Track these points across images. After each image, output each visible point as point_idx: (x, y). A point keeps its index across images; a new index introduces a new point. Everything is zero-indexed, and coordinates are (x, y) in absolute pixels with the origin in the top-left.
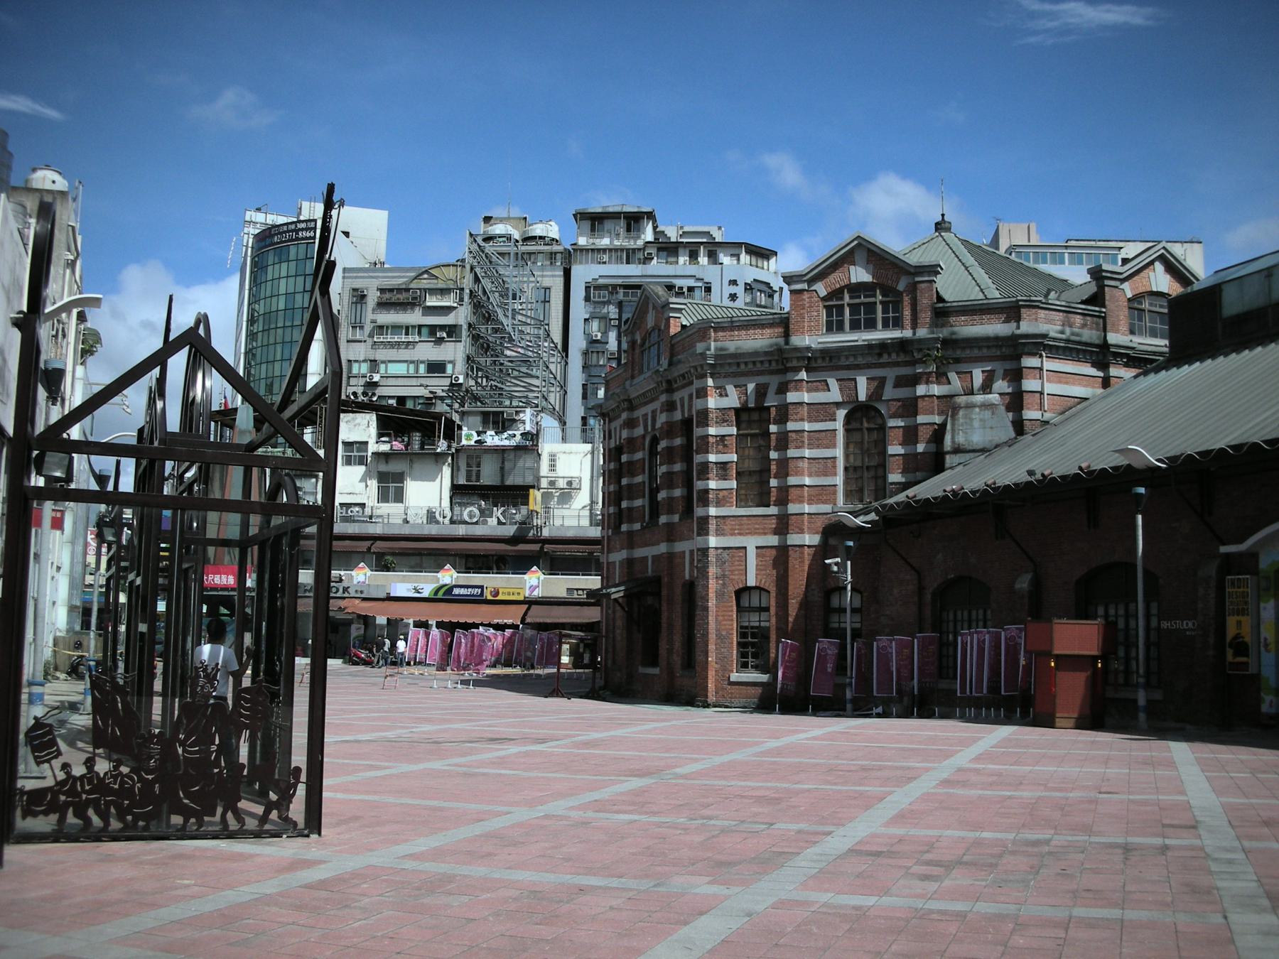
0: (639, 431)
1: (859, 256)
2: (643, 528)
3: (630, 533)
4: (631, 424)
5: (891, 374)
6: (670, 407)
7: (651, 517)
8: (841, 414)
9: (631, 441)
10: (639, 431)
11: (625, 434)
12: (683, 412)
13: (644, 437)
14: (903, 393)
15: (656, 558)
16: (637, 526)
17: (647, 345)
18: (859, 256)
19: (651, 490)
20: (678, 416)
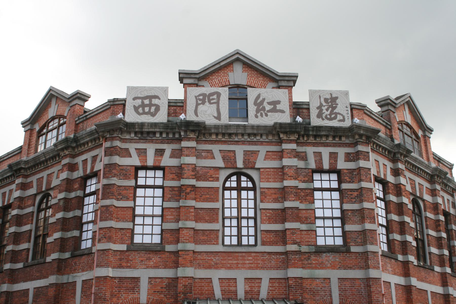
0: (32, 191)
1: (238, 68)
2: (25, 267)
3: (12, 271)
4: (24, 187)
5: (263, 150)
6: (72, 167)
7: (33, 259)
8: (223, 174)
9: (20, 199)
10: (32, 191)
11: (17, 194)
12: (85, 169)
13: (35, 195)
14: (274, 164)
15: (38, 290)
16: (20, 265)
17: (45, 131)
18: (238, 68)
19: (37, 237)
20: (79, 173)
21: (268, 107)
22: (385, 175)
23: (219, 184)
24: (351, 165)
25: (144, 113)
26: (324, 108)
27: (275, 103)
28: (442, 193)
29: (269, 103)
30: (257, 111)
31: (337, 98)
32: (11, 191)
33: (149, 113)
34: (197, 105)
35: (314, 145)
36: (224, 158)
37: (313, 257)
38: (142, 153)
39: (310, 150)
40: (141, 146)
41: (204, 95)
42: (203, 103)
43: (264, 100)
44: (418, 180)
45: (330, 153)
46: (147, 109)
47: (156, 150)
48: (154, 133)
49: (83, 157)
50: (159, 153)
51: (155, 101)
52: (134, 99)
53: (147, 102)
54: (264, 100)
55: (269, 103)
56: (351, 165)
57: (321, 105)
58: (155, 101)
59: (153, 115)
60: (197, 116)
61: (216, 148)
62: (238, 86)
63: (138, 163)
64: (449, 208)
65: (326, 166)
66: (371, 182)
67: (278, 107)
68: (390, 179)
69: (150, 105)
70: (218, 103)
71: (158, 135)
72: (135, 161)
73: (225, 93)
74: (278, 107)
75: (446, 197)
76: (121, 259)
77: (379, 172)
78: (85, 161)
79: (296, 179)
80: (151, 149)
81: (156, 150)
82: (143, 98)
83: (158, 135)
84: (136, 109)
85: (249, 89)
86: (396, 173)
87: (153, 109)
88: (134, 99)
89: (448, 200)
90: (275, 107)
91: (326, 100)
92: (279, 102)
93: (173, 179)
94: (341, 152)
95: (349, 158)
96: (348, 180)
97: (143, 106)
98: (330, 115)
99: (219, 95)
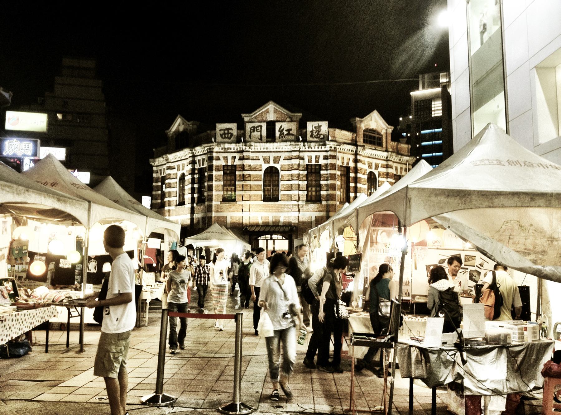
5: (283, 155)
20: (197, 166)
21: (286, 133)
22: (348, 163)
23: (262, 173)
24: (325, 162)
25: (225, 138)
26: (314, 132)
27: (289, 130)
28: (394, 165)
29: (286, 131)
30: (280, 135)
31: (321, 126)
32: (164, 169)
33: (228, 138)
34: (251, 133)
35: (308, 151)
36: (264, 159)
37: (304, 206)
38: (226, 158)
39: (306, 155)
40: (225, 155)
41: (254, 127)
42: (254, 132)
43: (283, 129)
44: (374, 161)
45: (316, 156)
46: (226, 136)
47: (232, 157)
48: (231, 149)
49: (199, 158)
50: (234, 158)
51: (230, 131)
52: (220, 130)
53: (226, 132)
54: (283, 129)
55: (286, 131)
56: (325, 162)
57: (313, 130)
58: (230, 131)
59: (230, 138)
60: (250, 138)
61: (260, 155)
62: (271, 121)
63: (224, 164)
64: (401, 172)
65: (313, 163)
66: (335, 170)
67: (291, 132)
68: (352, 165)
69: (228, 133)
70: (261, 131)
71: (232, 149)
72: (222, 163)
73: (264, 125)
74: (291, 132)
75: (399, 166)
76: (218, 208)
77: (343, 163)
78: (199, 161)
79: (297, 169)
80: (230, 156)
81: (232, 157)
82: (224, 130)
83: (232, 149)
84: (221, 135)
85: (277, 124)
86: (356, 161)
87: (229, 135)
88: (220, 130)
89: (401, 168)
90: (289, 132)
91: (315, 127)
92: (291, 130)
93: (240, 171)
94: (322, 155)
95: (326, 158)
96: (324, 168)
97: (225, 134)
98: (317, 135)
99: (261, 126)
